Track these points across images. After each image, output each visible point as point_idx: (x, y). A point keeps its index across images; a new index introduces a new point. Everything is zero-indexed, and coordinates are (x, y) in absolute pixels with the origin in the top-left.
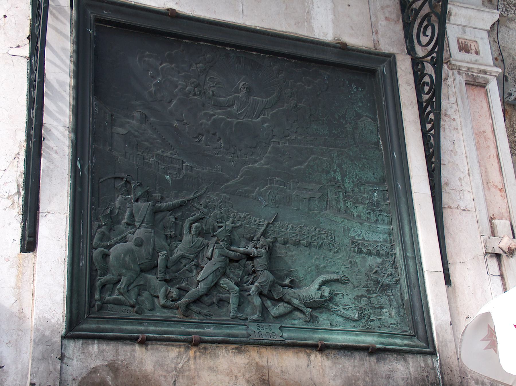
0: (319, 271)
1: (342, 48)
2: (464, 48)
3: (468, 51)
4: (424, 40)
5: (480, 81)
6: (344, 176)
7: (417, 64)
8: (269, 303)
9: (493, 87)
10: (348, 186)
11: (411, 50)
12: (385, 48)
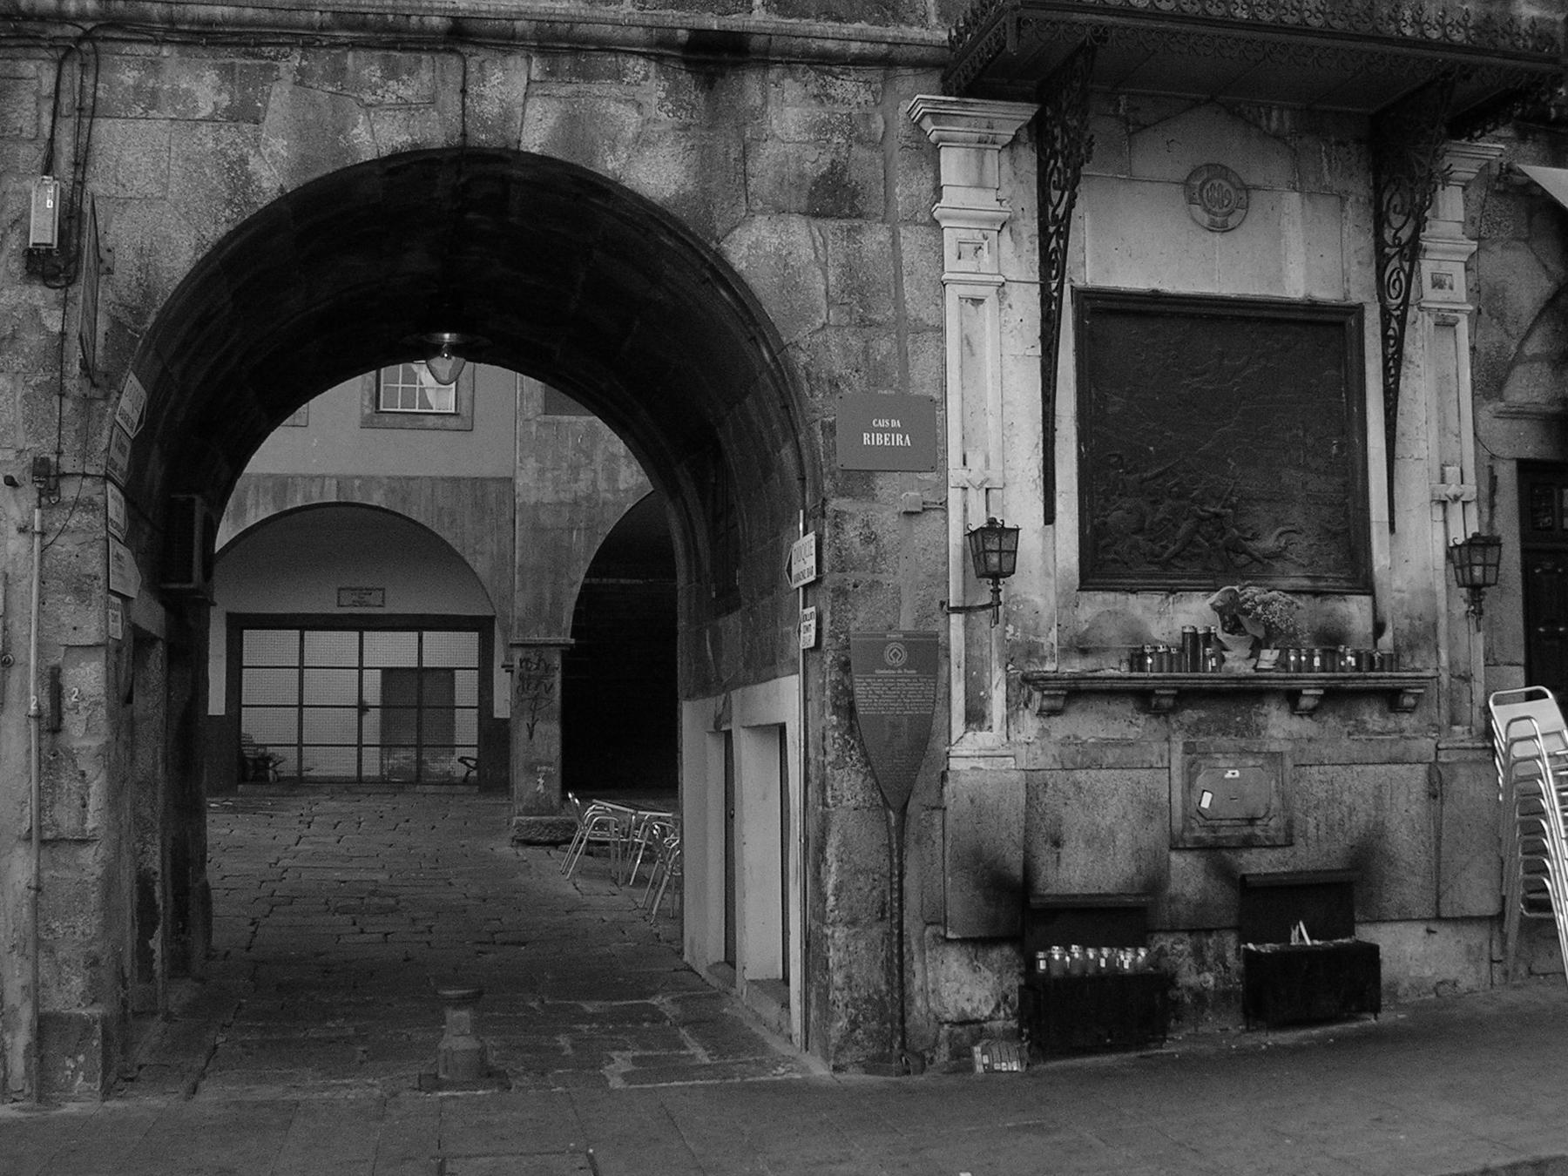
0: (1278, 523)
1: (1312, 306)
2: (1438, 284)
3: (1441, 287)
4: (1394, 293)
5: (1451, 321)
6: (1306, 431)
7: (1385, 314)
8: (1232, 555)
9: (1463, 326)
10: (1310, 441)
11: (1382, 300)
12: (1355, 298)
